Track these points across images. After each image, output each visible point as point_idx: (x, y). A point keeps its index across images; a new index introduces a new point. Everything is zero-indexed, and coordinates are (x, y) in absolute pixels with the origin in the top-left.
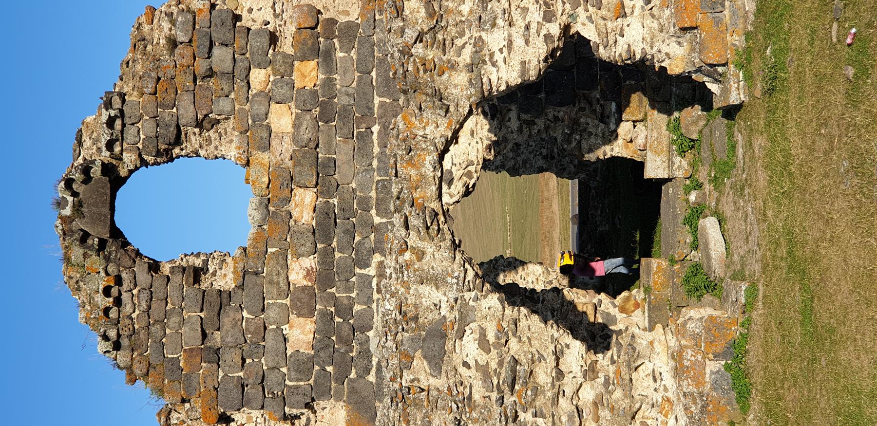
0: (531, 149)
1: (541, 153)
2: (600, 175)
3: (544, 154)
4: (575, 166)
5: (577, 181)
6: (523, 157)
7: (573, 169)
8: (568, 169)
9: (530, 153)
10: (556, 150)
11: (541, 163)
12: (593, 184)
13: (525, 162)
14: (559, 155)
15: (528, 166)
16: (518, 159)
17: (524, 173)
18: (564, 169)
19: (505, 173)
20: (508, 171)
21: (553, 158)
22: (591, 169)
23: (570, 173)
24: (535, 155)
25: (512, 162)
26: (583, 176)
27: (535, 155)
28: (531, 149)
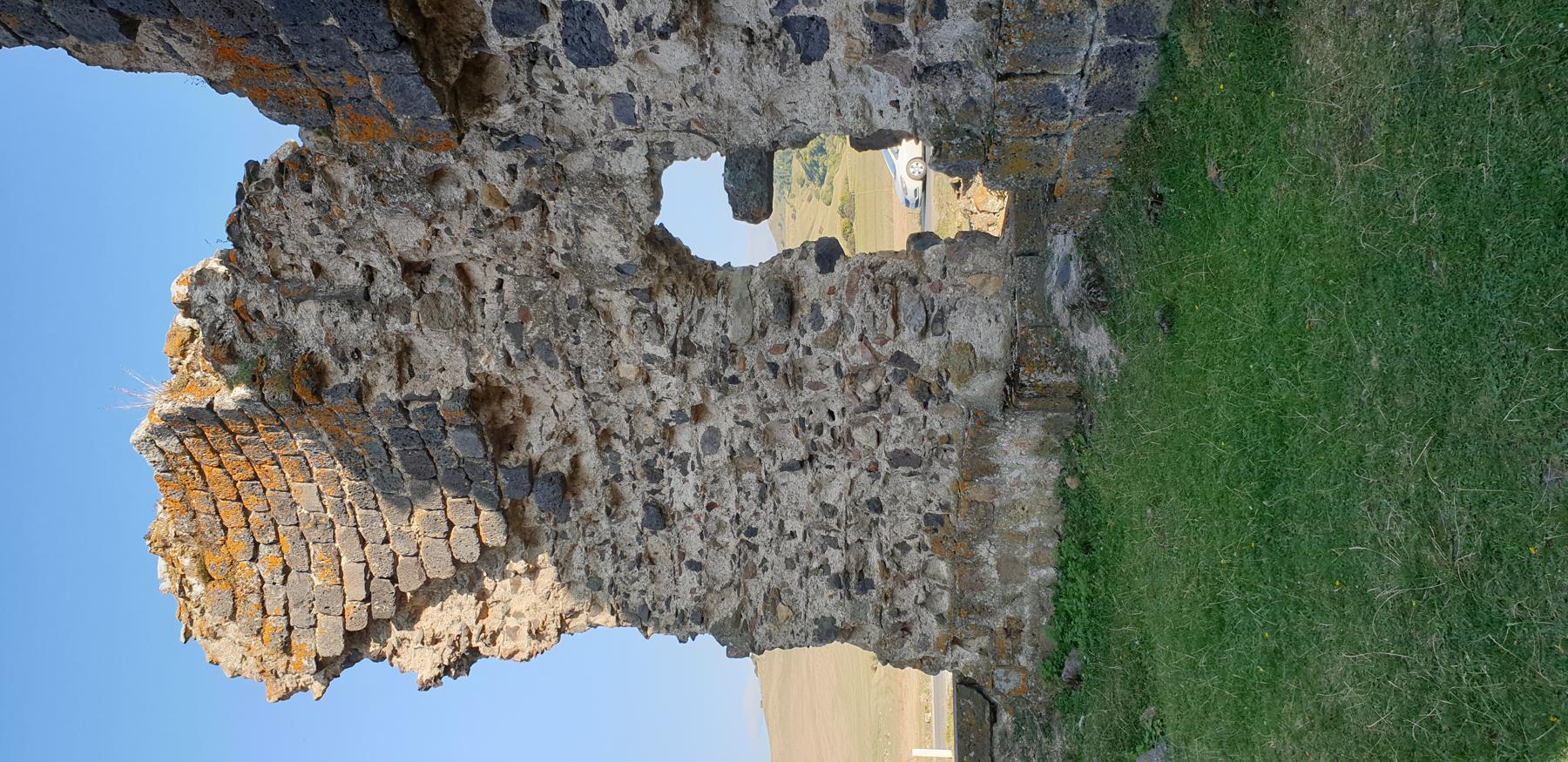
0: (790, 547)
1: (825, 567)
2: (1028, 648)
3: (837, 566)
4: (940, 618)
5: (947, 676)
6: (766, 578)
7: (935, 630)
8: (917, 631)
9: (790, 564)
10: (874, 557)
11: (827, 602)
12: (1006, 683)
13: (773, 597)
14: (885, 570)
15: (783, 610)
16: (751, 583)
17: (772, 641)
18: (906, 629)
19: (706, 640)
20: (719, 634)
21: (865, 585)
22: (998, 624)
23: (924, 645)
24: (807, 572)
25: (732, 601)
26: (968, 656)
27: (807, 572)
28: (790, 547)
